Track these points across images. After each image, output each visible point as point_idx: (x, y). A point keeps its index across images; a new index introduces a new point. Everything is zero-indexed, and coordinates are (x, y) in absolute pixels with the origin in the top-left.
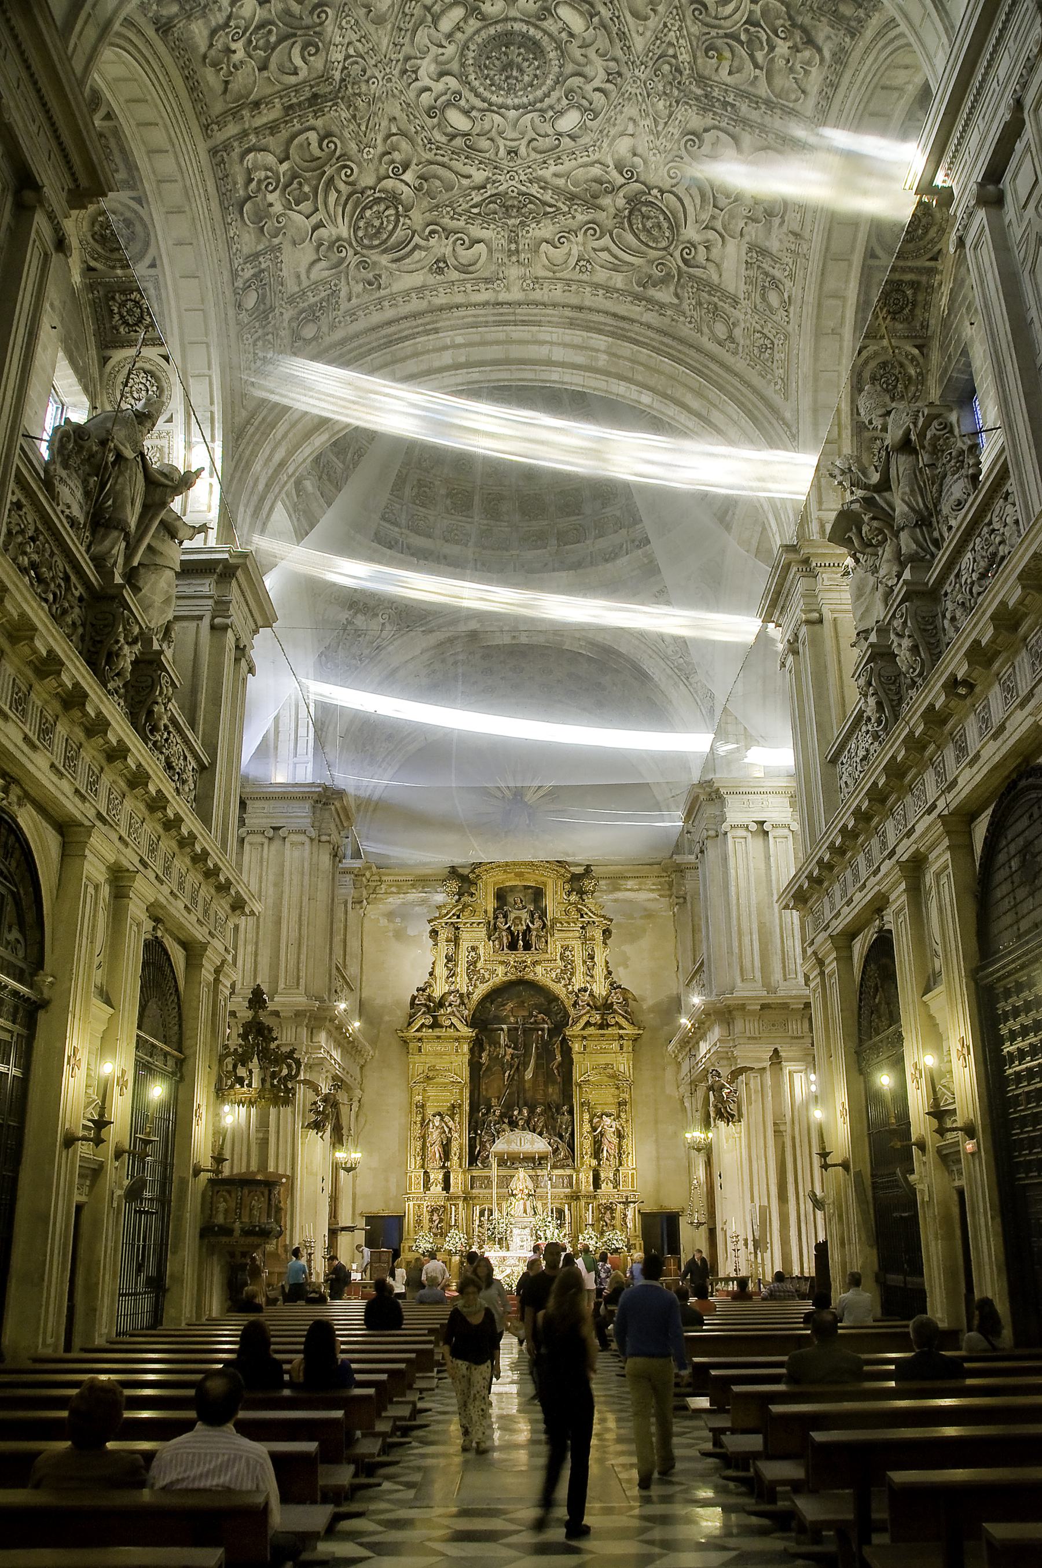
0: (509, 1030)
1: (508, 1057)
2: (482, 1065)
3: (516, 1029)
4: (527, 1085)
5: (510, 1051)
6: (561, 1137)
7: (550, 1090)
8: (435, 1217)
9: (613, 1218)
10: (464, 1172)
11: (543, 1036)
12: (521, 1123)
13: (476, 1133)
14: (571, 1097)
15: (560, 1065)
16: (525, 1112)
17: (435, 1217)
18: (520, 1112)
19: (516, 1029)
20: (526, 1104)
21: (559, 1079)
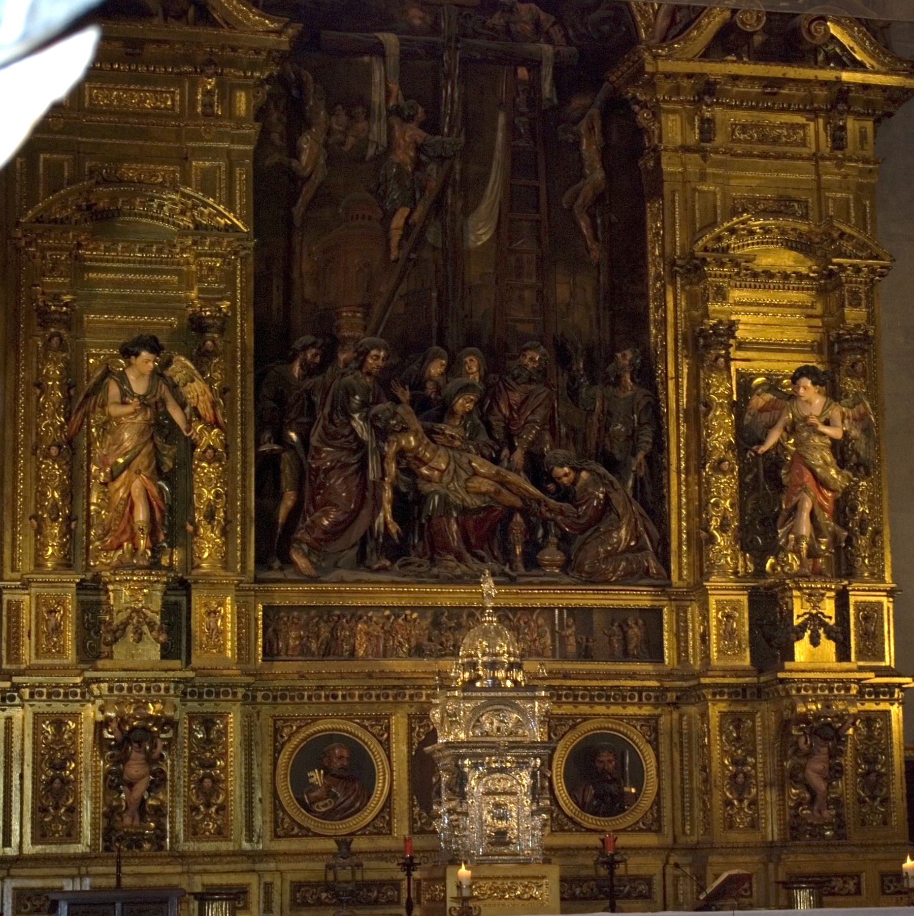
0: (406, 56)
1: (404, 156)
2: (295, 180)
3: (433, 51)
4: (475, 271)
5: (410, 134)
6: (612, 464)
7: (562, 292)
8: (135, 768)
9: (835, 772)
10: (240, 591)
11: (534, 86)
12: (463, 404)
13: (280, 438)
14: (639, 321)
15: (599, 198)
16: (473, 366)
17: (135, 768)
18: (453, 367)
19: (433, 51)
20: (471, 339)
21: (596, 253)
